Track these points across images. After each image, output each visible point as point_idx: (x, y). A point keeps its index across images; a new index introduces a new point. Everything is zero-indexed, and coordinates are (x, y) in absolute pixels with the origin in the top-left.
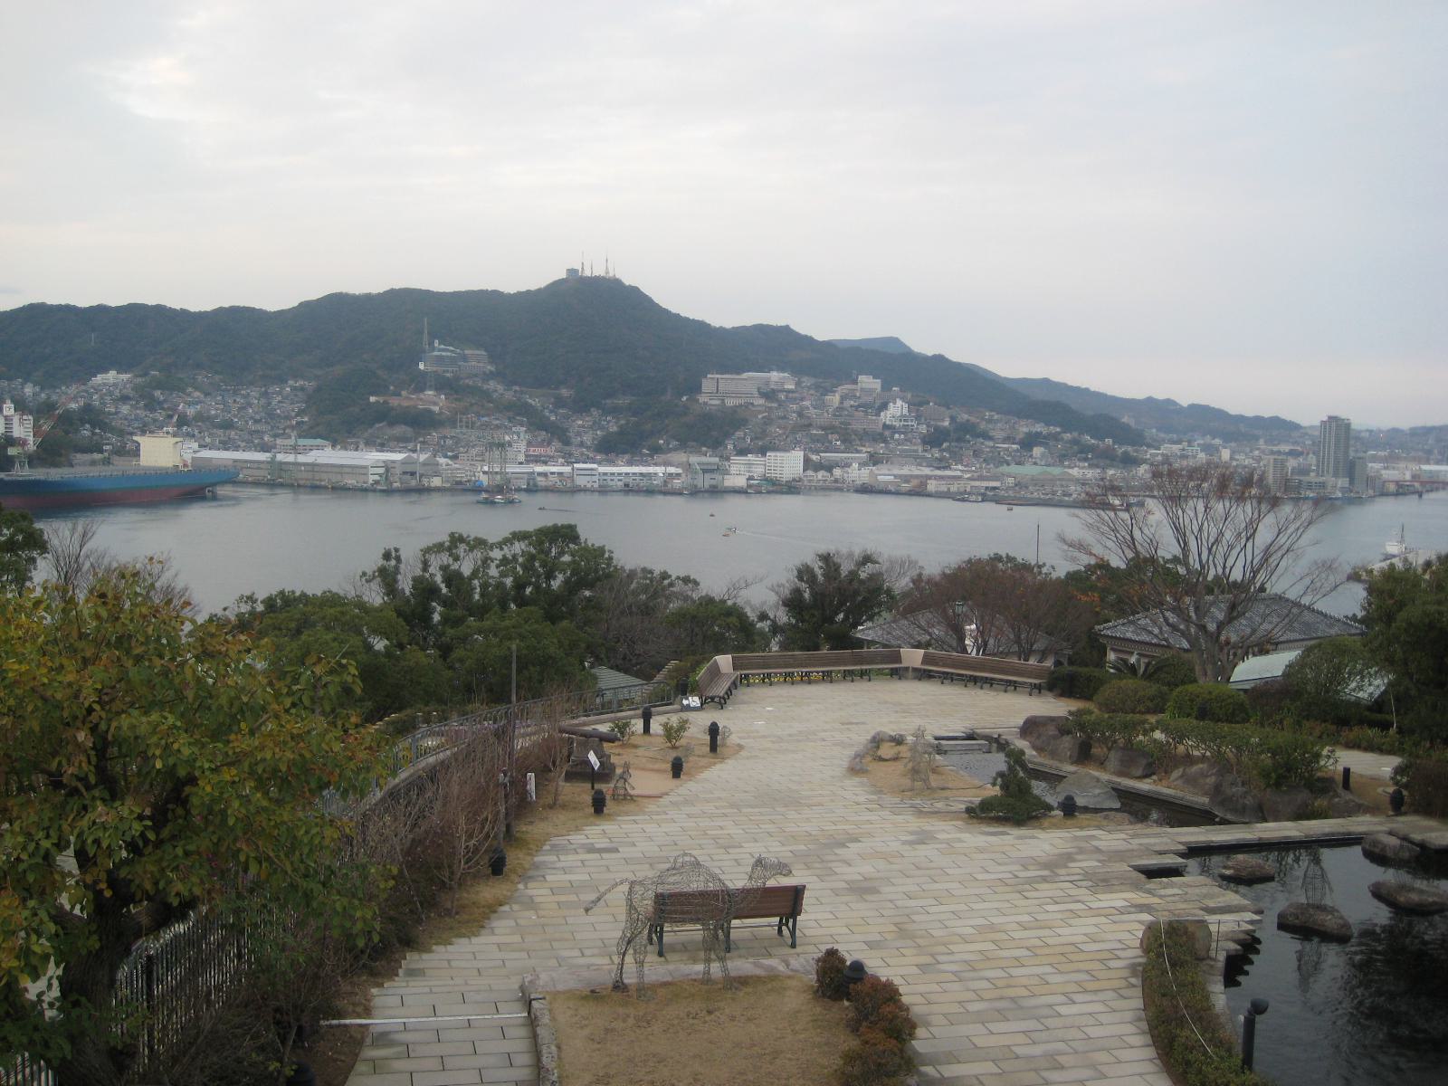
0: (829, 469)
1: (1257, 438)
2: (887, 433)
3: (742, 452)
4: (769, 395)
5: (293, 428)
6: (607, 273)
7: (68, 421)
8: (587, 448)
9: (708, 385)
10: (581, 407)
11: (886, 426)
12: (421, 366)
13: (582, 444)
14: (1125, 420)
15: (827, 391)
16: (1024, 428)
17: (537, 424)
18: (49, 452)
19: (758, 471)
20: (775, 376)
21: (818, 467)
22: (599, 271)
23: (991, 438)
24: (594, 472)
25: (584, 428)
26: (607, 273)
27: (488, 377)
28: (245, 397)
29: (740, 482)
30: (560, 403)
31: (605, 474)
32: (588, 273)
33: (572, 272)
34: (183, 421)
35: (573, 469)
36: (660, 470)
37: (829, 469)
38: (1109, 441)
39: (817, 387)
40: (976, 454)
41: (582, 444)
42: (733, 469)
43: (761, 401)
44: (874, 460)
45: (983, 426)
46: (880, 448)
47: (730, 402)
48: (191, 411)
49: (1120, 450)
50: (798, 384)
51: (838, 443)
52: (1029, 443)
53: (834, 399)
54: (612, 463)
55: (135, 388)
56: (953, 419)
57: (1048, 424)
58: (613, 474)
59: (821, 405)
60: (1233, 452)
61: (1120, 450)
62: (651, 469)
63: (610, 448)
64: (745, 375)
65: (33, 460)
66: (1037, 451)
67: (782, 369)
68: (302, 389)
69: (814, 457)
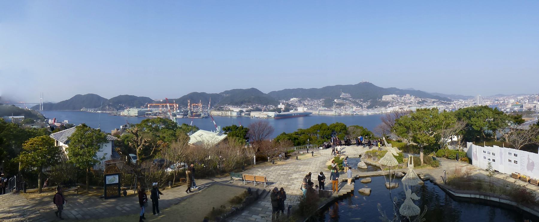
0: (403, 109)
1: (468, 99)
2: (411, 103)
3: (389, 107)
4: (393, 98)
5: (321, 106)
7: (289, 105)
8: (365, 108)
9: (383, 97)
10: (364, 102)
11: (411, 102)
12: (341, 96)
13: (364, 107)
14: (448, 98)
15: (402, 97)
16: (433, 100)
17: (357, 104)
18: (287, 110)
20: (394, 95)
21: (401, 109)
23: (427, 102)
25: (365, 105)
27: (350, 98)
28: (314, 101)
30: (361, 101)
34: (305, 105)
38: (446, 101)
39: (400, 96)
40: (425, 105)
41: (364, 107)
45: (426, 100)
46: (410, 105)
47: (387, 99)
48: (306, 104)
49: (447, 102)
50: (397, 96)
52: (434, 102)
53: (403, 98)
55: (298, 100)
56: (422, 100)
57: (436, 99)
59: (401, 99)
60: (465, 102)
61: (447, 102)
63: (368, 108)
64: (390, 95)
65: (284, 111)
66: (435, 104)
67: (394, 94)
68: (323, 100)
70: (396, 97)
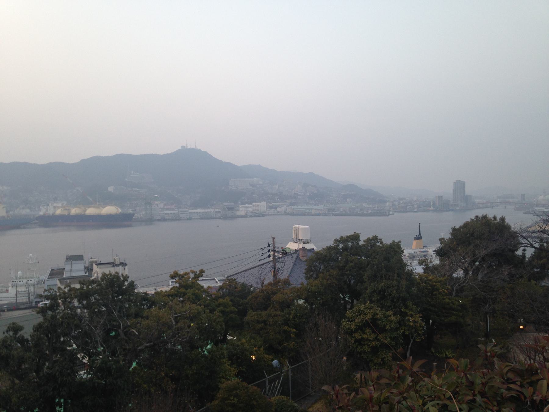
0: (276, 208)
3: (243, 204)
6: (196, 147)
19: (250, 210)
21: (271, 208)
22: (193, 146)
24: (187, 212)
26: (196, 147)
29: (243, 213)
31: (191, 213)
32: (189, 147)
33: (183, 147)
35: (179, 211)
36: (212, 211)
37: (276, 208)
42: (241, 210)
43: (251, 187)
44: (291, 204)
51: (278, 199)
54: (196, 209)
58: (195, 213)
62: (209, 210)
69: (270, 204)
70: (261, 183)
